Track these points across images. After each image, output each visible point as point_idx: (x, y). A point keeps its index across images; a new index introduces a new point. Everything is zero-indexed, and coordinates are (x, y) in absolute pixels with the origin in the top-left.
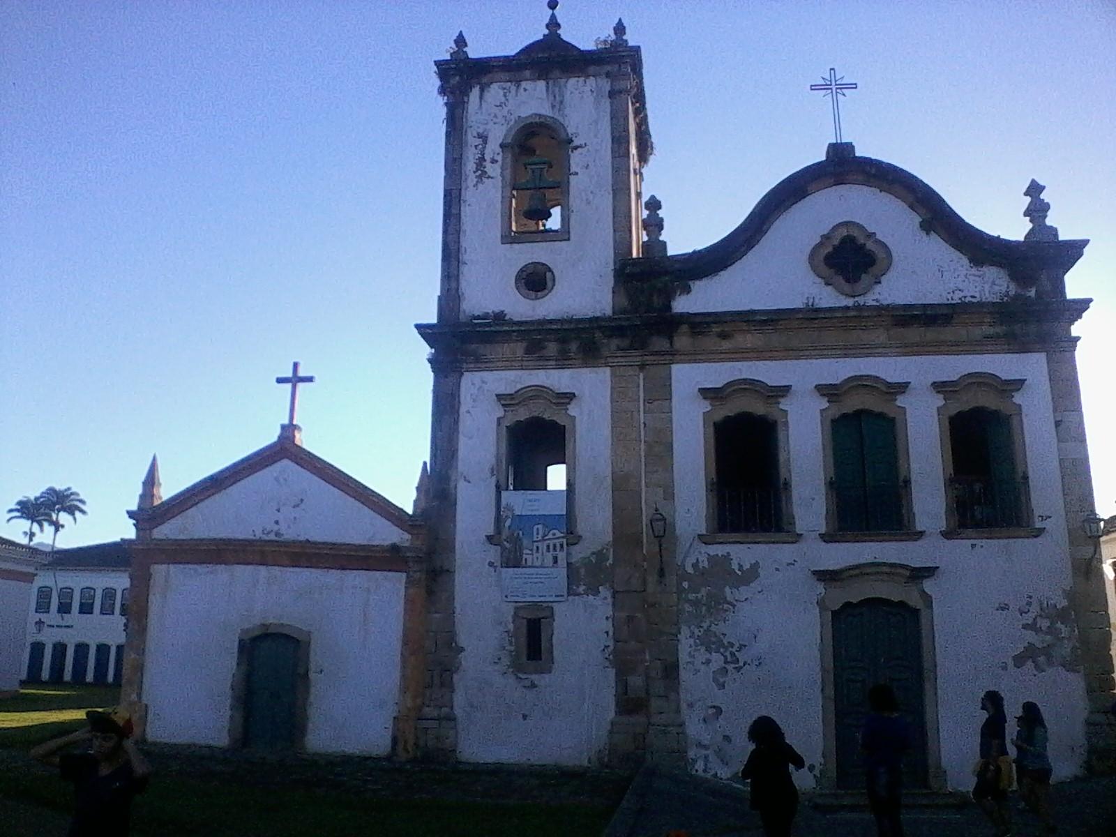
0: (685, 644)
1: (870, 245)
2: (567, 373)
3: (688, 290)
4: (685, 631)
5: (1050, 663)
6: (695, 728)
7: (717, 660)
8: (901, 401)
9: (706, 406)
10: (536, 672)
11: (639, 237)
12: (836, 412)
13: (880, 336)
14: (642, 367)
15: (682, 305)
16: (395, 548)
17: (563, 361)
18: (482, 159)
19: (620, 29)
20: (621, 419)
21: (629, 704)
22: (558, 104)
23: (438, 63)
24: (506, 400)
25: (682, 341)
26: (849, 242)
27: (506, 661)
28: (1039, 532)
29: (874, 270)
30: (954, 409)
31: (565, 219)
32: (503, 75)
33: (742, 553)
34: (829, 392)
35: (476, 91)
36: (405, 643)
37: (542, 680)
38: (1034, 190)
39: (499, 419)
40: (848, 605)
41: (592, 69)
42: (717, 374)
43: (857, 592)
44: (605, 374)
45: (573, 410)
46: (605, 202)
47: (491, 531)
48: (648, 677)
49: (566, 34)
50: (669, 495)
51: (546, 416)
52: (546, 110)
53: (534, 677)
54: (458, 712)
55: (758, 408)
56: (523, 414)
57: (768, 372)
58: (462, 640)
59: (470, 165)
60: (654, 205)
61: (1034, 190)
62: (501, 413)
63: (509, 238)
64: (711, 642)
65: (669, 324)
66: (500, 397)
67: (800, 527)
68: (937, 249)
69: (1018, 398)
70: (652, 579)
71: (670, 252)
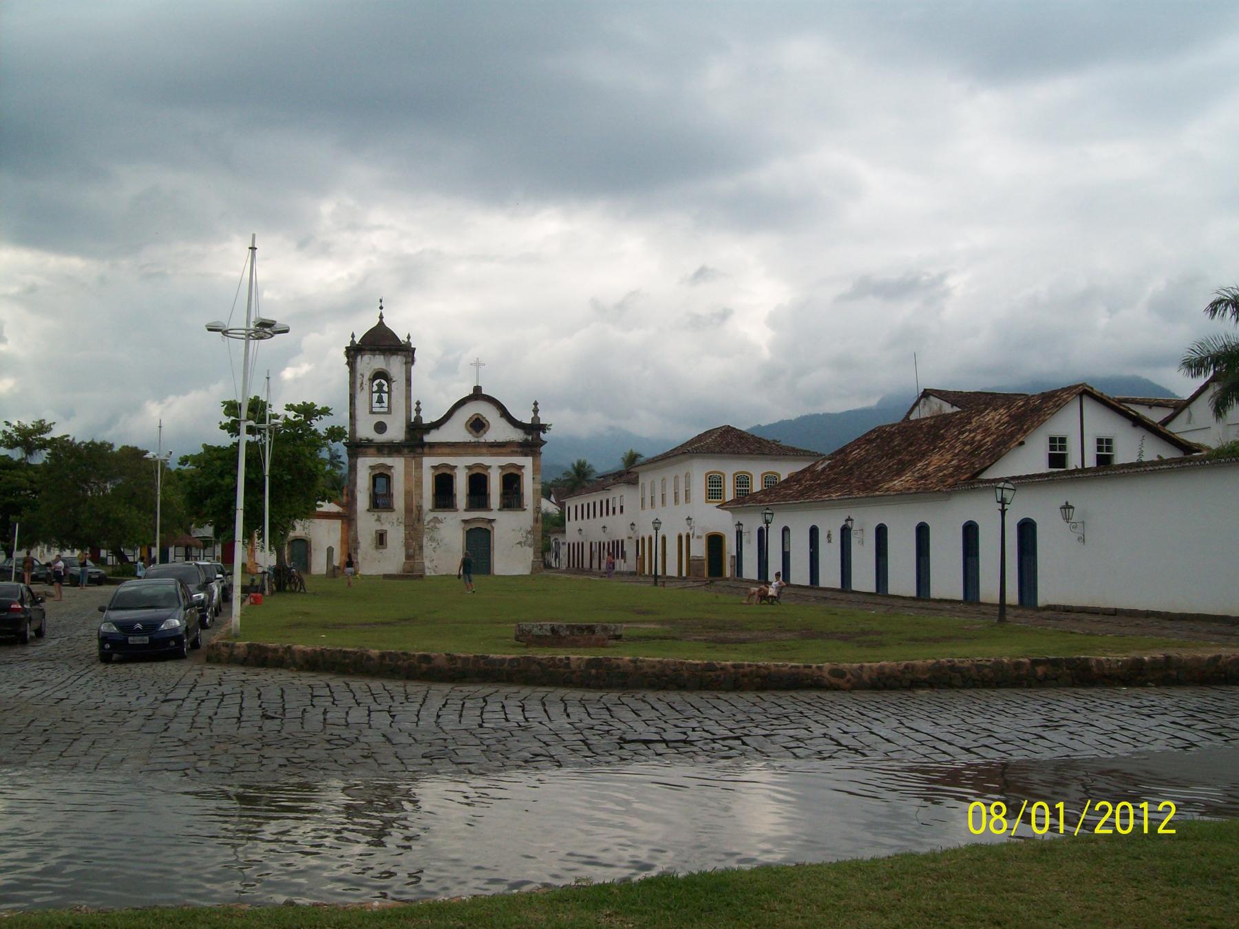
0: (425, 540)
1: (484, 422)
2: (391, 459)
3: (429, 433)
4: (425, 536)
5: (525, 545)
6: (427, 563)
7: (434, 544)
8: (489, 471)
9: (433, 471)
10: (383, 548)
11: (414, 414)
12: (470, 473)
13: (484, 450)
14: (414, 457)
15: (428, 438)
16: (338, 513)
17: (390, 455)
18: (362, 383)
19: (409, 337)
20: (407, 474)
21: (409, 557)
22: (388, 364)
23: (347, 348)
24: (372, 468)
25: (426, 450)
26: (478, 419)
27: (374, 546)
28: (525, 510)
29: (485, 429)
30: (505, 473)
31: (389, 407)
32: (369, 352)
33: (441, 515)
34: (469, 468)
35: (359, 358)
36: (342, 541)
37: (384, 551)
38: (536, 404)
39: (370, 474)
40: (471, 529)
41: (400, 353)
42: (437, 461)
43: (473, 526)
44: (402, 460)
45: (393, 471)
46: (403, 401)
47: (367, 508)
48: (415, 550)
49: (388, 323)
50: (421, 498)
51: (385, 472)
52: (384, 367)
53: (381, 550)
54: (360, 562)
55: (448, 472)
56: (377, 472)
57: (451, 461)
58: (360, 539)
59: (358, 385)
60: (418, 403)
61: (536, 404)
62: (370, 471)
63: (372, 412)
64: (432, 539)
65: (423, 445)
66: (370, 467)
67: (458, 507)
68: (503, 423)
69: (523, 471)
70: (416, 522)
71: (424, 422)
